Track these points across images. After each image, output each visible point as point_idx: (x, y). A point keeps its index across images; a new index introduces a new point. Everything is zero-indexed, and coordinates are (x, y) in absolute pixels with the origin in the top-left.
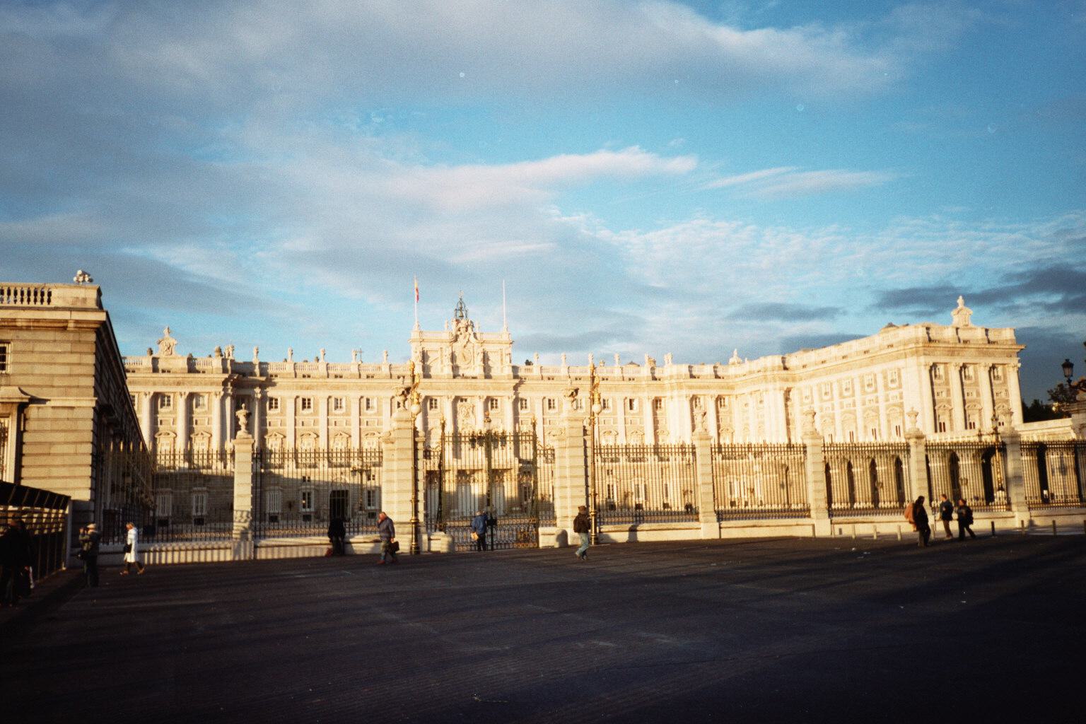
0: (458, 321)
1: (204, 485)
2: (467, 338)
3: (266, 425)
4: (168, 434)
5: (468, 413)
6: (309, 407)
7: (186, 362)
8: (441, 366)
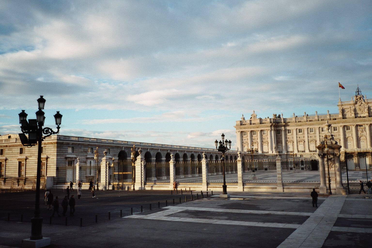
0: (357, 96)
1: (266, 158)
2: (361, 102)
3: (287, 139)
4: (256, 143)
5: (363, 130)
6: (301, 132)
7: (259, 121)
8: (351, 114)
